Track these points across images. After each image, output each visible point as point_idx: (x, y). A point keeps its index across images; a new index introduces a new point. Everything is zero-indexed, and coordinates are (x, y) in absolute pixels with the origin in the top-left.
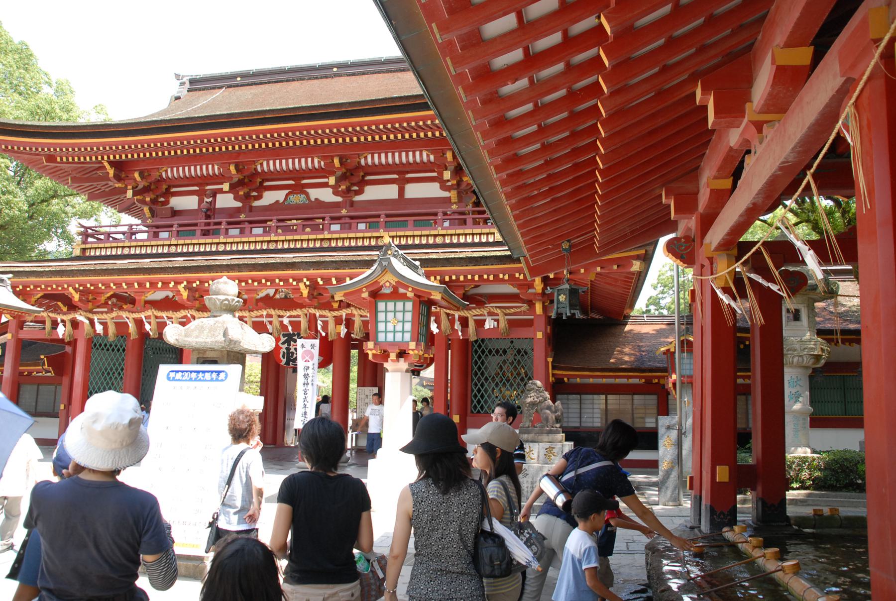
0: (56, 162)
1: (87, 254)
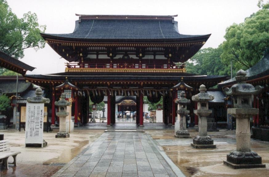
1: (69, 71)
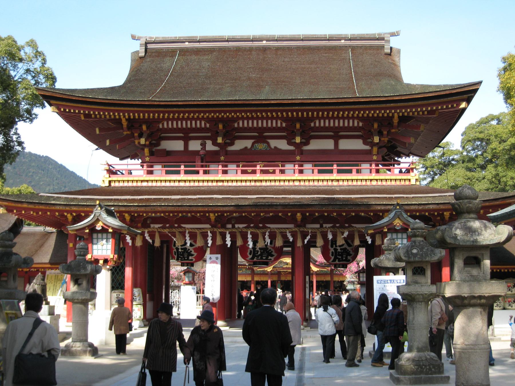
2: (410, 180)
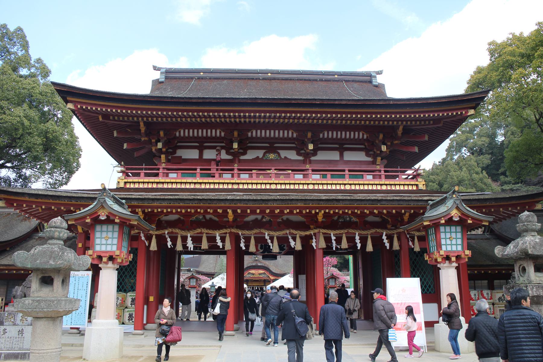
0: (109, 119)
2: (417, 185)
